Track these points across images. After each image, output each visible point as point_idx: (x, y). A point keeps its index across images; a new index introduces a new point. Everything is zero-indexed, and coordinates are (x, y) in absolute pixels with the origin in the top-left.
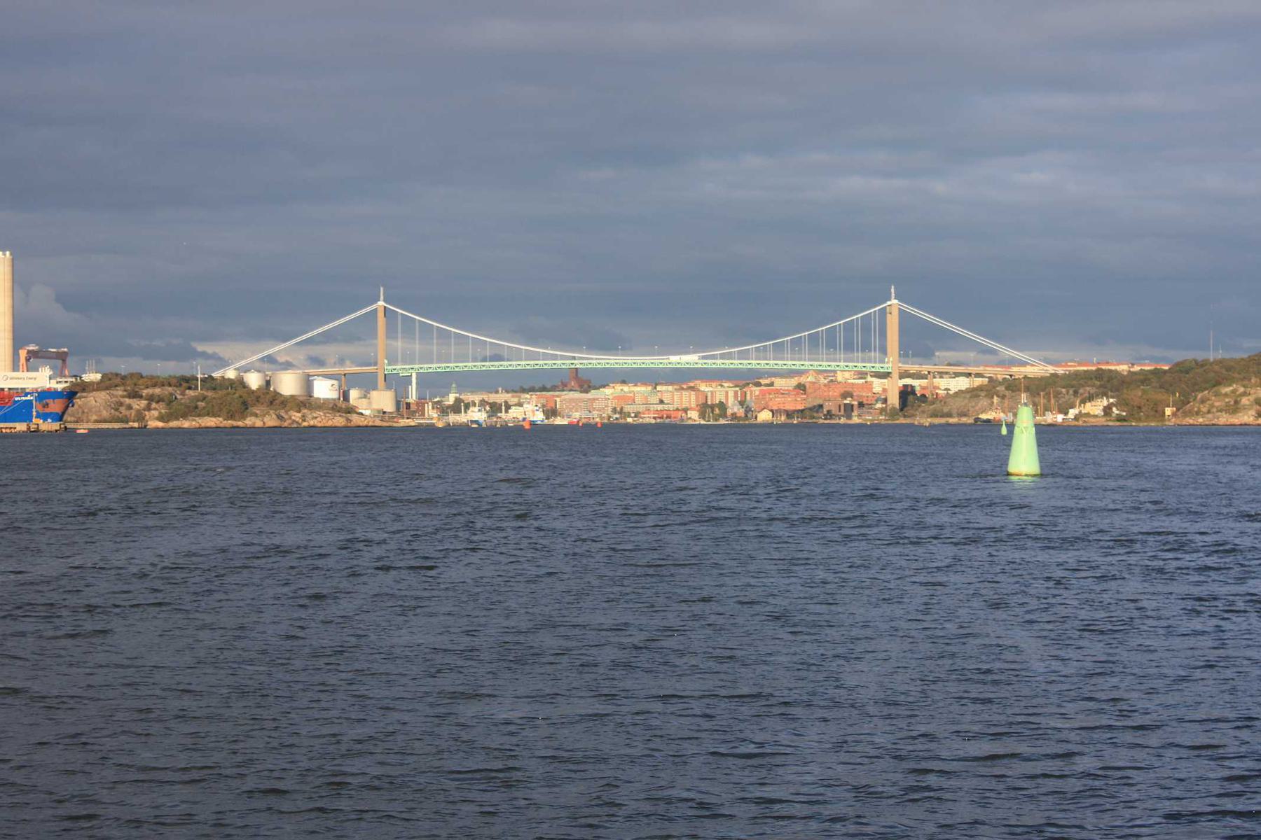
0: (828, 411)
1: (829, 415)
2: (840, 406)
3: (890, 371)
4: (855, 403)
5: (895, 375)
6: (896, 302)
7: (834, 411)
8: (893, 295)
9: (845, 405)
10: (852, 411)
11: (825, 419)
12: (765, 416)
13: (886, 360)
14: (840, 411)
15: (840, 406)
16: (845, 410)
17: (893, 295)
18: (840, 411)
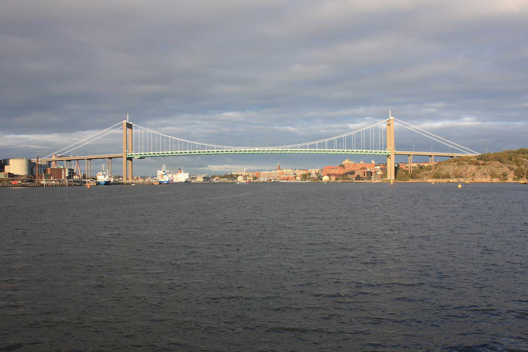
0: (358, 176)
1: (358, 178)
2: (364, 172)
3: (390, 154)
4: (373, 171)
5: (393, 157)
6: (392, 118)
7: (361, 175)
8: (390, 115)
9: (367, 171)
10: (372, 175)
11: (357, 180)
12: (326, 178)
13: (387, 149)
14: (364, 176)
15: (364, 172)
16: (367, 175)
17: (390, 115)
18: (364, 176)
